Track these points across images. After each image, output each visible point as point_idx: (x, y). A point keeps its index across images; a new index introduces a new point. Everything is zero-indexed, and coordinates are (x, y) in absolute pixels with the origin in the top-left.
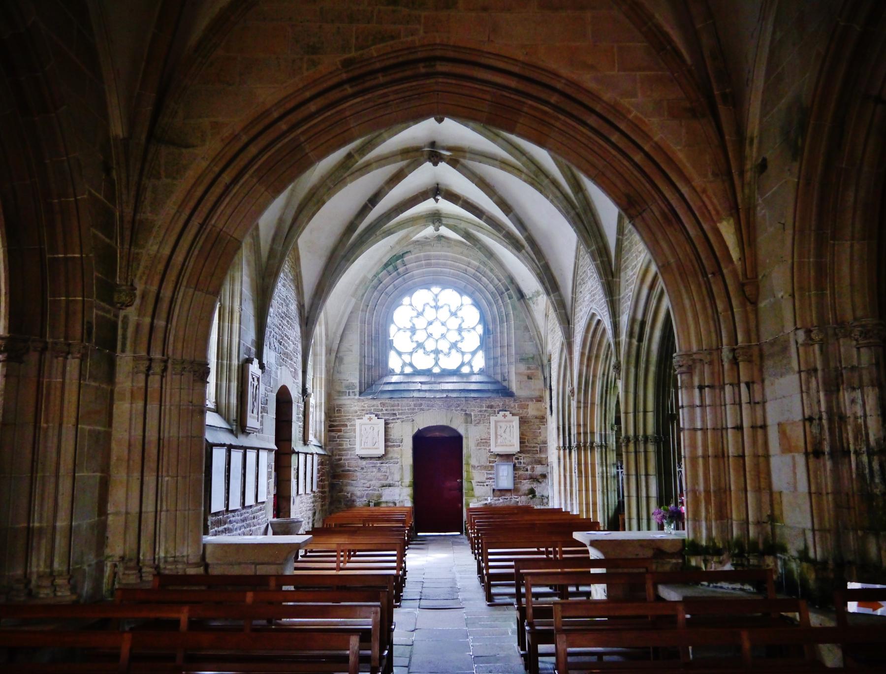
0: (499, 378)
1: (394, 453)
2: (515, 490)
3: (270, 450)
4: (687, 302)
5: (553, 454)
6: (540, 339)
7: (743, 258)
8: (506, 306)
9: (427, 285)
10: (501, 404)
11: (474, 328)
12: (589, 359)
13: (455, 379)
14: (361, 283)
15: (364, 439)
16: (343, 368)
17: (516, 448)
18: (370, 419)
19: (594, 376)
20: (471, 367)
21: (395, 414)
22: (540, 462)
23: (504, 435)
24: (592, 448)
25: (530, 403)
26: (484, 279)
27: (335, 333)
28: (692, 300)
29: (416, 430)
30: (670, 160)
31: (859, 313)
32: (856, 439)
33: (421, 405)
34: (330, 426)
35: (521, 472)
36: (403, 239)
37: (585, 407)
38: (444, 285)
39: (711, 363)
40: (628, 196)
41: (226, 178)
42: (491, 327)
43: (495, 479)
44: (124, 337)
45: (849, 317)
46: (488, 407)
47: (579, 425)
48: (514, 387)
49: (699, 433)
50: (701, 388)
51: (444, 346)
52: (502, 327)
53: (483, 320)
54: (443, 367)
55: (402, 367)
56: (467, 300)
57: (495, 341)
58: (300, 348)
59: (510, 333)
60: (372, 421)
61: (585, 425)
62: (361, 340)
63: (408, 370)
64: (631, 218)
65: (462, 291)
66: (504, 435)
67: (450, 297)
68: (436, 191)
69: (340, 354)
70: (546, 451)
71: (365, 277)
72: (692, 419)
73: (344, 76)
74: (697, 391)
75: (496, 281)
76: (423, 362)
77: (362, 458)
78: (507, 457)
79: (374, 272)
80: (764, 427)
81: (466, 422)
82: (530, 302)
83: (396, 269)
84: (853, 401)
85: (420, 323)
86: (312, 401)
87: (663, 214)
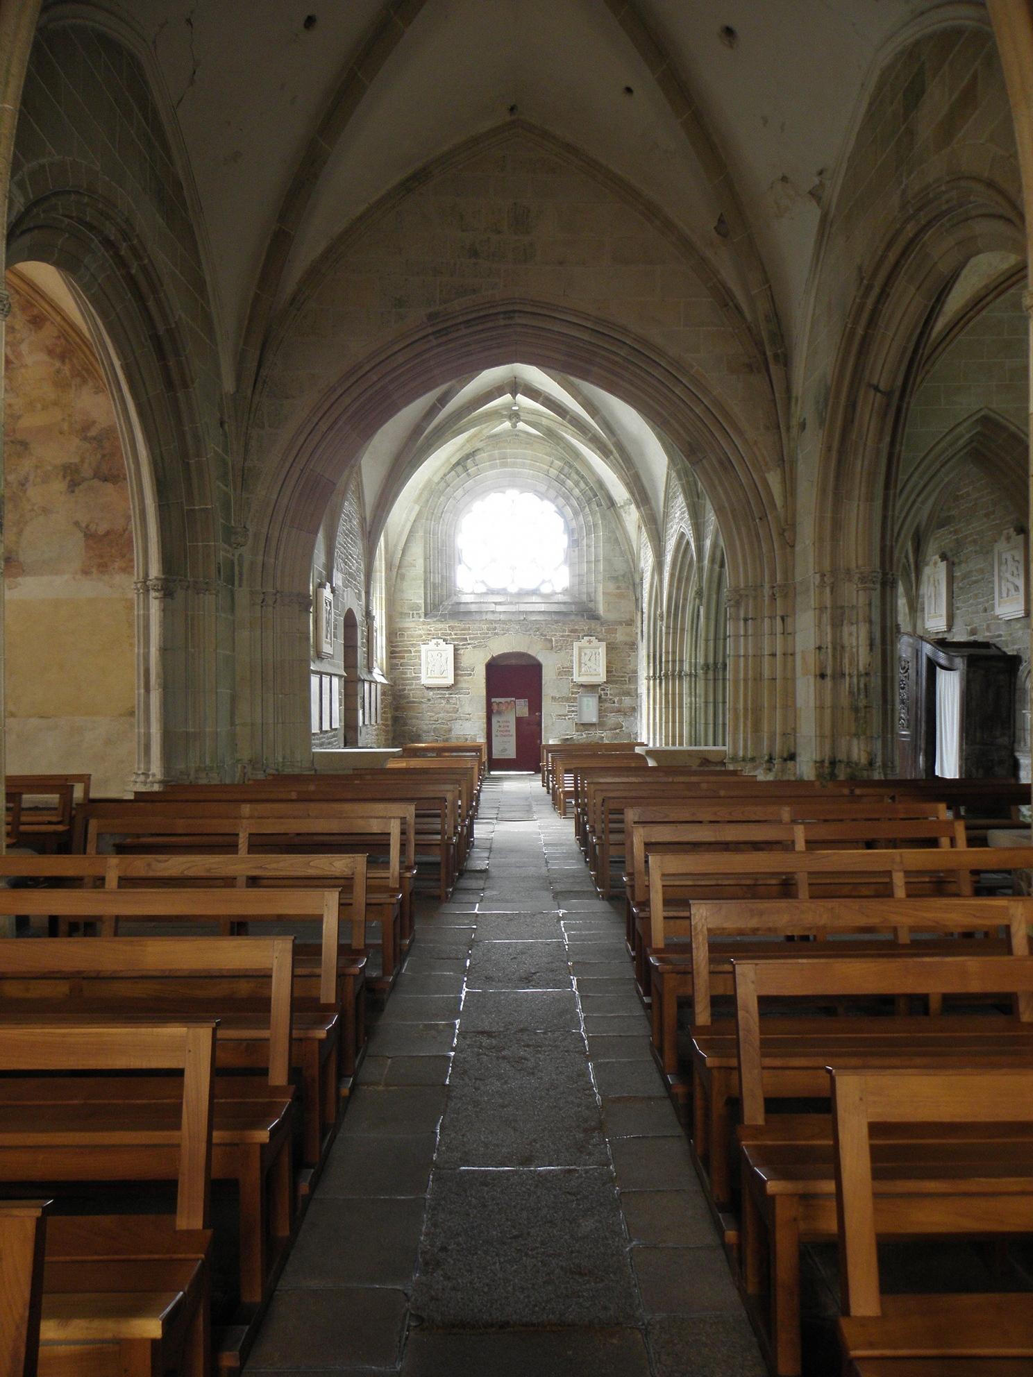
0: (584, 597)
2: (600, 725)
3: (340, 676)
4: (737, 543)
5: (643, 686)
6: (632, 553)
7: (785, 506)
13: (534, 599)
17: (601, 677)
18: (437, 644)
19: (685, 599)
22: (628, 694)
23: (589, 664)
24: (680, 677)
25: (619, 627)
28: (741, 540)
30: (726, 414)
31: (860, 562)
32: (851, 664)
34: (392, 652)
35: (607, 705)
36: (475, 435)
37: (675, 633)
39: (755, 598)
40: (690, 444)
41: (323, 427)
43: (579, 712)
44: (241, 574)
45: (853, 565)
48: (601, 609)
49: (742, 659)
50: (746, 620)
58: (362, 567)
61: (674, 652)
65: (542, 496)
66: (589, 664)
68: (515, 386)
70: (636, 682)
71: (430, 480)
72: (737, 648)
73: (430, 330)
74: (742, 622)
78: (591, 688)
80: (793, 654)
84: (851, 634)
87: (721, 463)
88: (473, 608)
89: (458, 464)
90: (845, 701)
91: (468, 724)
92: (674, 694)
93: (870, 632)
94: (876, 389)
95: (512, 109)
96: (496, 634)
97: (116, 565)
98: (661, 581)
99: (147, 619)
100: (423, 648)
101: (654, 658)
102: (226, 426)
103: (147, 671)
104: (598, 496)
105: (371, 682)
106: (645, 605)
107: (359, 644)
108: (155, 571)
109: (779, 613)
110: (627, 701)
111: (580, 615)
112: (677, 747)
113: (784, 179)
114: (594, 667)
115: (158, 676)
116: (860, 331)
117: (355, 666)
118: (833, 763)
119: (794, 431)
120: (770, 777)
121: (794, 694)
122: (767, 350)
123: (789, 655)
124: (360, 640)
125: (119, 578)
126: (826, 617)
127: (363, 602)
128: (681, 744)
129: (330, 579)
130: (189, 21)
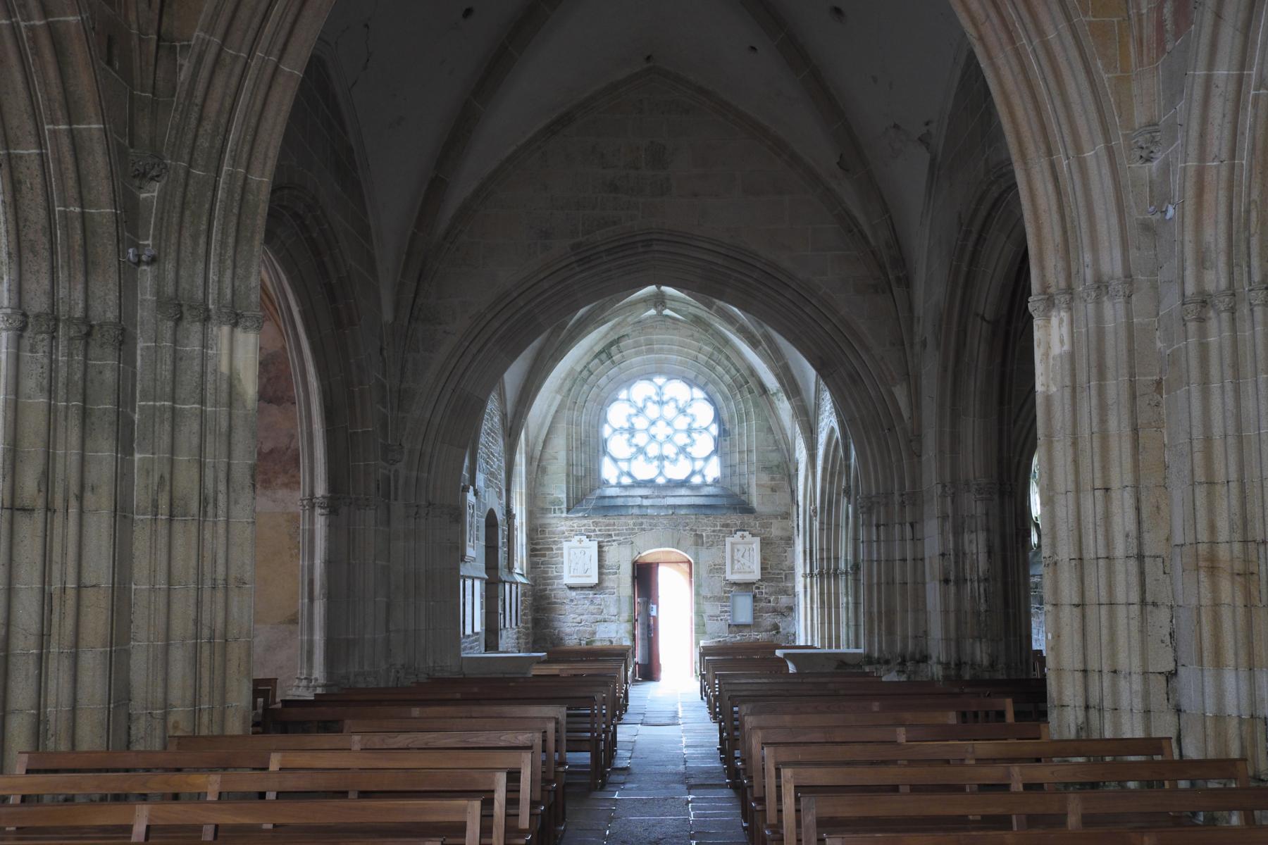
0: (737, 490)
1: (610, 582)
4: (868, 452)
6: (787, 444)
8: (745, 402)
9: (648, 376)
10: (738, 523)
11: (706, 429)
12: (832, 475)
13: (683, 491)
14: (568, 375)
17: (756, 575)
18: (581, 541)
20: (704, 476)
22: (785, 592)
24: (836, 576)
26: (719, 368)
27: (537, 437)
33: (641, 524)
34: (533, 550)
37: (829, 529)
38: (671, 376)
39: (887, 505)
42: (727, 427)
43: (732, 613)
44: (396, 489)
45: (971, 476)
46: (723, 526)
47: (822, 549)
48: (755, 502)
50: (878, 526)
51: (670, 450)
52: (741, 427)
53: (718, 418)
54: (669, 476)
55: (618, 478)
56: (698, 393)
57: (732, 445)
58: (503, 465)
59: (749, 434)
61: (829, 550)
62: (568, 446)
63: (626, 481)
65: (691, 383)
67: (678, 390)
69: (544, 463)
70: (794, 579)
71: (572, 369)
72: (870, 553)
73: (573, 259)
75: (733, 371)
76: (644, 471)
77: (571, 588)
78: (746, 586)
79: (584, 362)
80: (922, 559)
81: (696, 544)
83: (610, 357)
84: (971, 542)
85: (640, 423)
86: (517, 522)
88: (620, 502)
89: (601, 352)
90: (967, 605)
91: (613, 627)
93: (988, 540)
94: (983, 318)
95: (648, 58)
97: (279, 481)
100: (566, 545)
101: (808, 553)
102: (385, 352)
103: (311, 582)
104: (748, 383)
105: (511, 583)
108: (321, 490)
109: (908, 519)
110: (784, 600)
112: (834, 650)
113: (896, 126)
114: (748, 564)
115: (322, 587)
116: (964, 268)
117: (496, 568)
118: (959, 665)
120: (903, 678)
121: (925, 597)
122: (890, 272)
123: (919, 560)
125: (281, 493)
126: (949, 525)
128: (838, 646)
129: (473, 481)
130: (367, 26)
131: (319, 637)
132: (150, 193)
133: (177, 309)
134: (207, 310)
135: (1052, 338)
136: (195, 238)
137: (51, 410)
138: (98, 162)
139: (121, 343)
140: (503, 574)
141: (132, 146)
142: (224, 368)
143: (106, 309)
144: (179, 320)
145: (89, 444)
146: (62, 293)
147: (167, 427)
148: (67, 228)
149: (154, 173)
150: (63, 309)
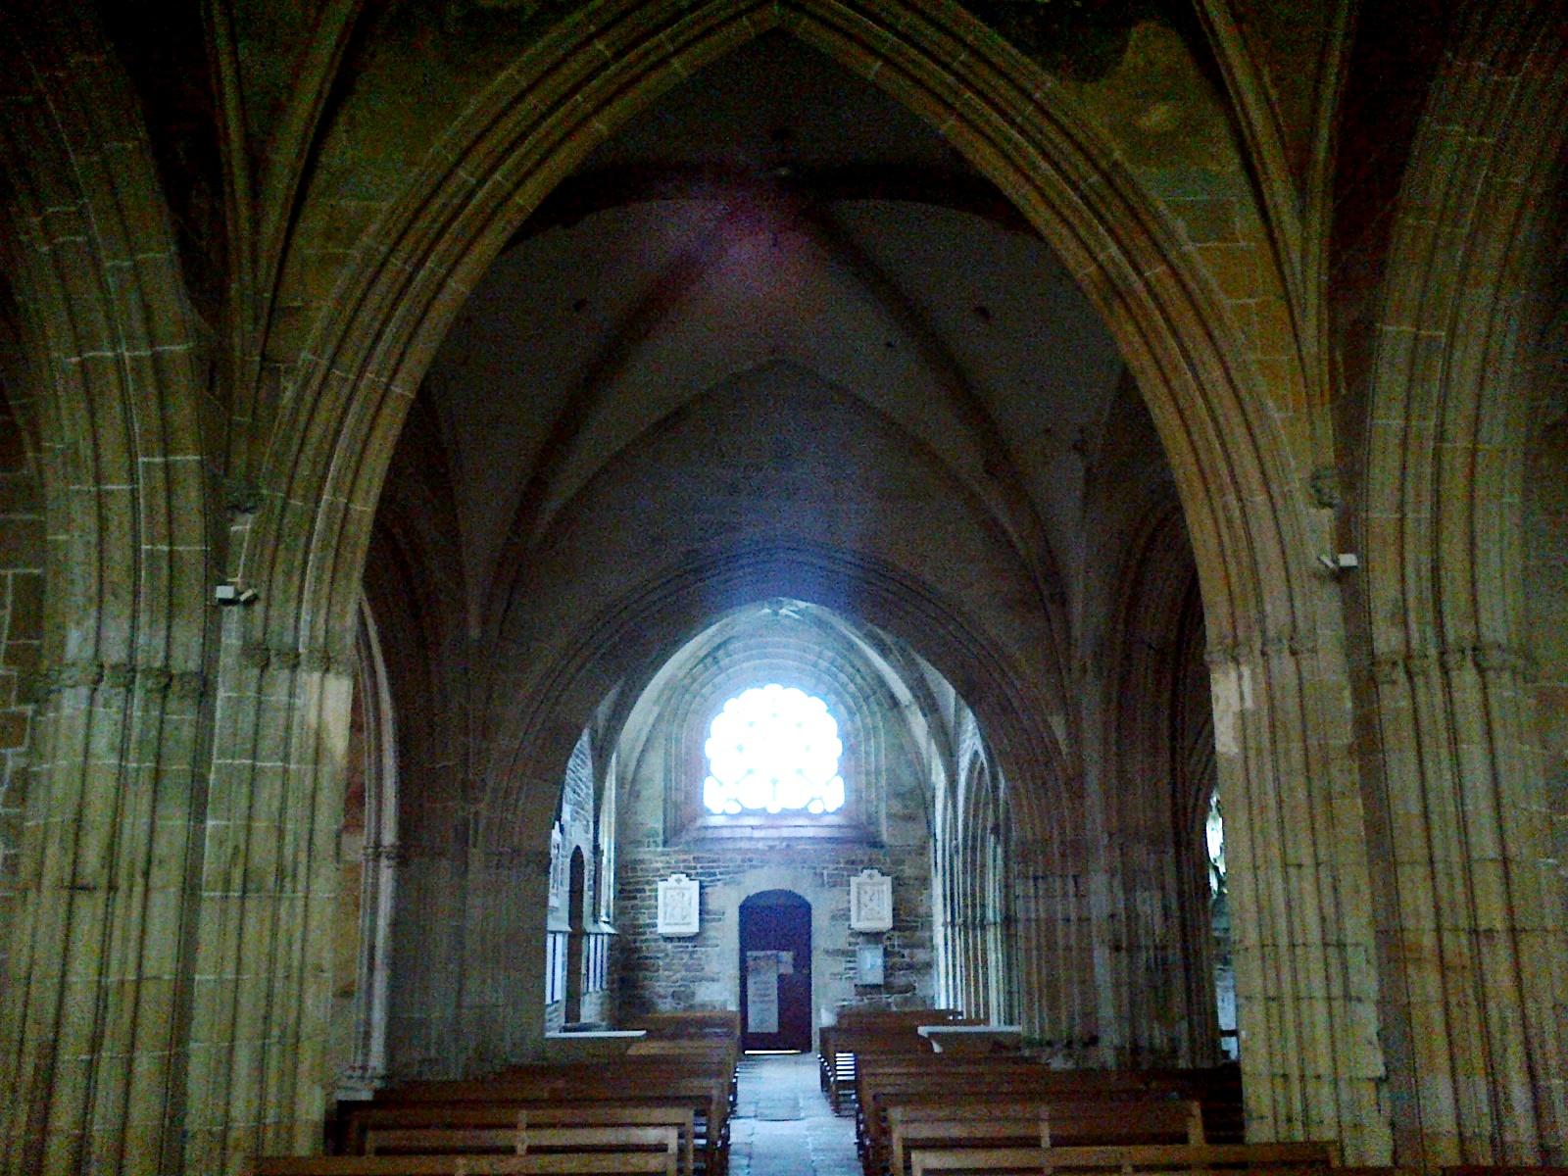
1: (712, 932)
2: (887, 987)
10: (866, 859)
15: (669, 909)
16: (640, 806)
17: (886, 922)
18: (679, 881)
21: (714, 874)
24: (983, 928)
29: (743, 898)
34: (621, 891)
35: (896, 959)
47: (965, 895)
48: (885, 837)
49: (1033, 924)
50: (1036, 879)
58: (591, 791)
60: (682, 884)
61: (973, 895)
62: (666, 765)
64: (972, 706)
65: (812, 692)
66: (871, 905)
69: (637, 788)
77: (668, 939)
78: (874, 937)
82: (907, 712)
83: (716, 661)
88: (726, 833)
89: (706, 657)
90: (1141, 978)
91: (716, 986)
92: (975, 949)
96: (755, 867)
98: (955, 812)
99: (376, 885)
100: (661, 885)
101: (950, 898)
103: (372, 948)
106: (939, 831)
107: (586, 888)
108: (389, 837)
111: (859, 844)
117: (581, 918)
119: (1076, 675)
124: (587, 883)
127: (591, 836)
131: (379, 1015)
132: (242, 526)
133: (260, 654)
134: (298, 656)
135: (1231, 693)
136: (288, 575)
137: (122, 772)
138: (191, 496)
139: (202, 695)
140: (589, 927)
141: (226, 475)
142: (312, 718)
143: (187, 661)
144: (265, 666)
145: (161, 811)
146: (142, 640)
147: (245, 789)
148: (154, 571)
149: (248, 505)
150: (140, 657)
